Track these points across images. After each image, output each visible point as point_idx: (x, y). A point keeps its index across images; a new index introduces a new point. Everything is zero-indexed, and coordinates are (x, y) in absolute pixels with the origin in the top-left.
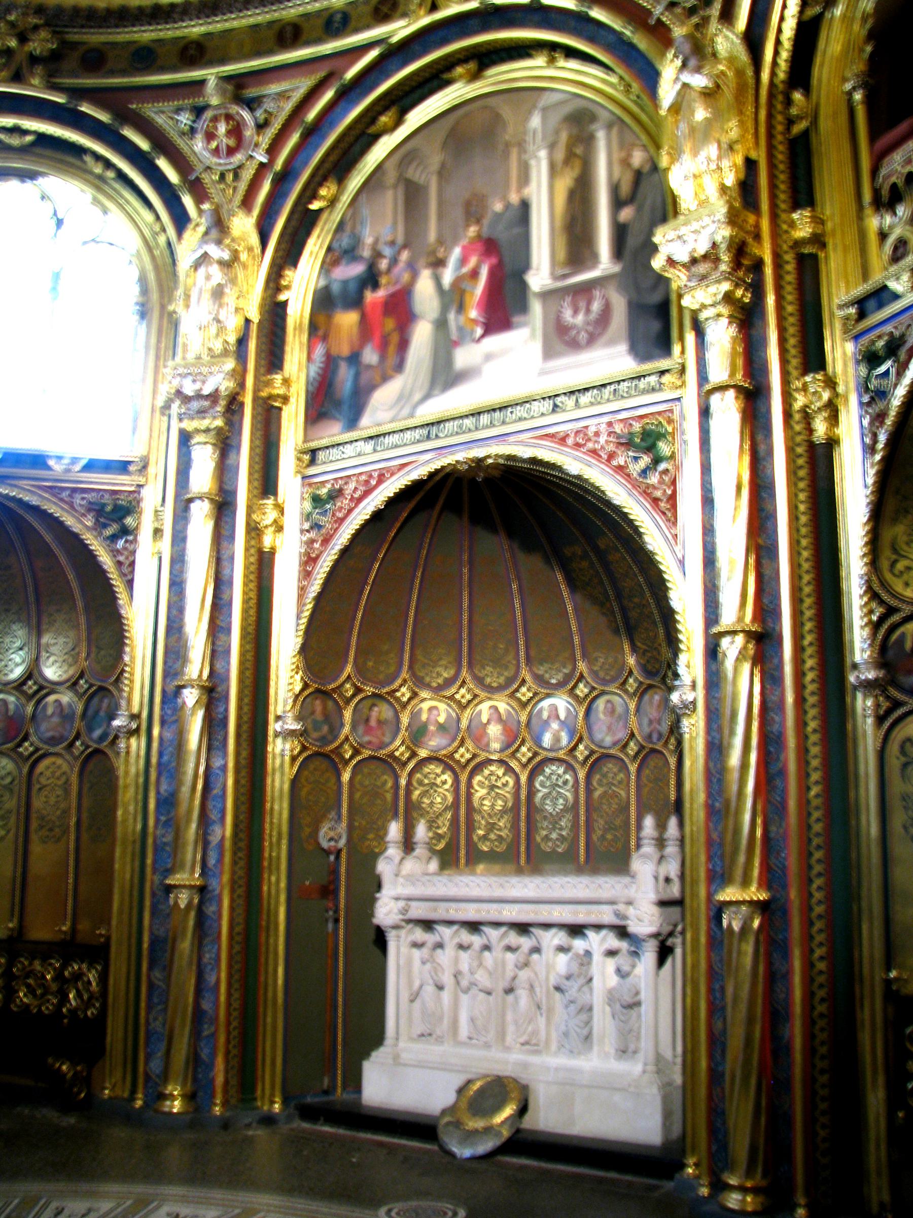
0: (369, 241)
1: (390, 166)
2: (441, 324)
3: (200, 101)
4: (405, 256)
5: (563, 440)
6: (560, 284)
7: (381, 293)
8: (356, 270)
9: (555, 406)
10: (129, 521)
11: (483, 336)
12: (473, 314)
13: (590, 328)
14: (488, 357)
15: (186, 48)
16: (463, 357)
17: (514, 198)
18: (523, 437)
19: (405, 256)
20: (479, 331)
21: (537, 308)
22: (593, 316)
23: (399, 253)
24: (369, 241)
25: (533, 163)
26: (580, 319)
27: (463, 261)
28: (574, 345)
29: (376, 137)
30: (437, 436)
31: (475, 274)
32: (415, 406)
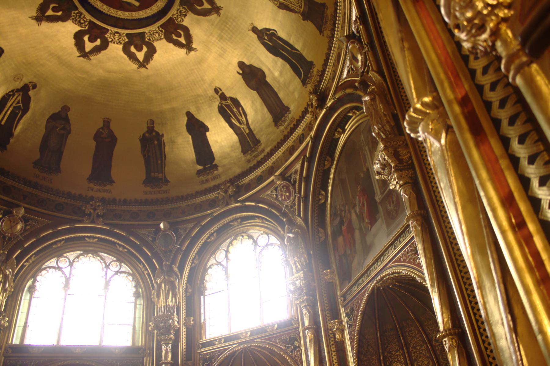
0: (338, 207)
1: (336, 178)
2: (360, 229)
3: (276, 186)
4: (347, 208)
5: (400, 261)
6: (384, 195)
7: (345, 225)
8: (338, 219)
9: (395, 246)
10: (296, 343)
11: (371, 227)
12: (367, 221)
13: (395, 208)
14: (374, 236)
15: (269, 170)
16: (369, 239)
17: (365, 170)
18: (390, 264)
19: (347, 208)
20: (370, 226)
21: (380, 208)
22: (395, 204)
23: (345, 207)
24: (338, 207)
25: (365, 152)
26: (392, 207)
27: (359, 201)
28: (394, 218)
29: (329, 170)
30: (370, 275)
31: (363, 205)
32: (362, 266)
